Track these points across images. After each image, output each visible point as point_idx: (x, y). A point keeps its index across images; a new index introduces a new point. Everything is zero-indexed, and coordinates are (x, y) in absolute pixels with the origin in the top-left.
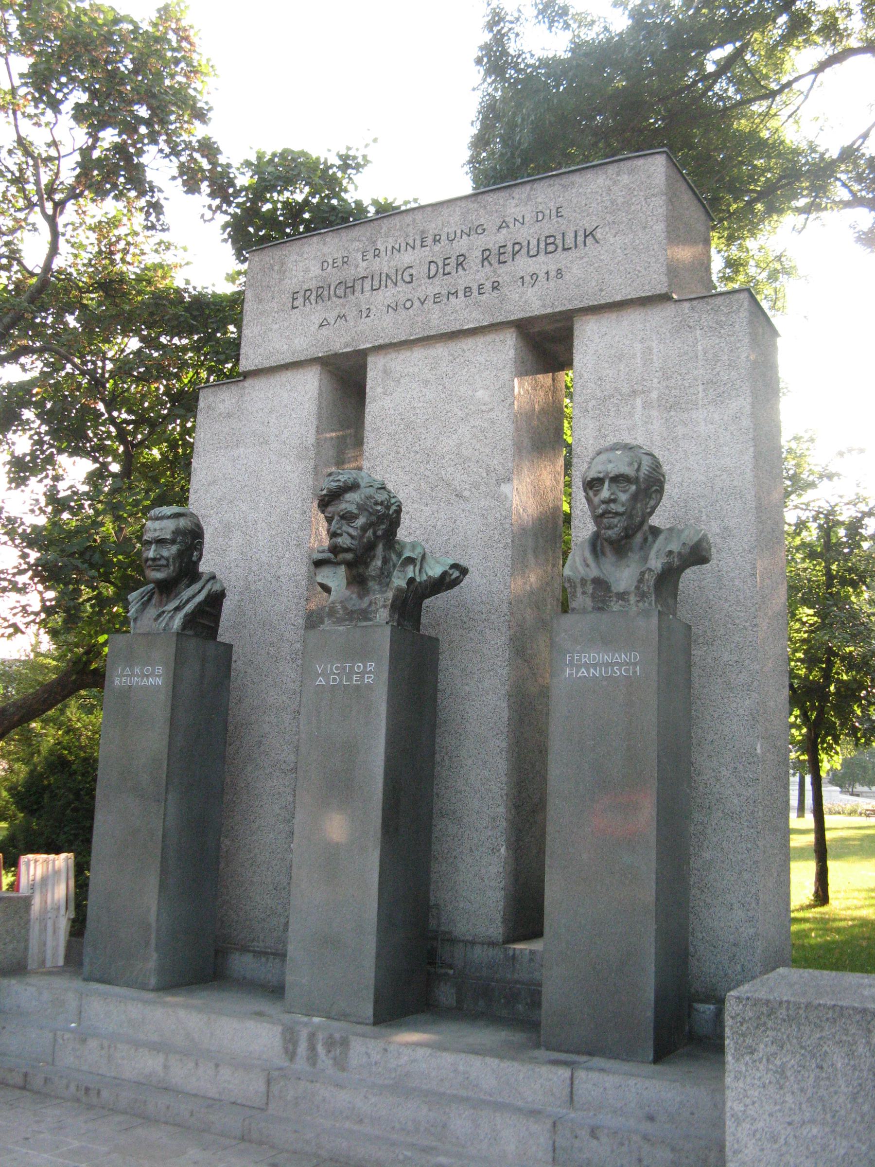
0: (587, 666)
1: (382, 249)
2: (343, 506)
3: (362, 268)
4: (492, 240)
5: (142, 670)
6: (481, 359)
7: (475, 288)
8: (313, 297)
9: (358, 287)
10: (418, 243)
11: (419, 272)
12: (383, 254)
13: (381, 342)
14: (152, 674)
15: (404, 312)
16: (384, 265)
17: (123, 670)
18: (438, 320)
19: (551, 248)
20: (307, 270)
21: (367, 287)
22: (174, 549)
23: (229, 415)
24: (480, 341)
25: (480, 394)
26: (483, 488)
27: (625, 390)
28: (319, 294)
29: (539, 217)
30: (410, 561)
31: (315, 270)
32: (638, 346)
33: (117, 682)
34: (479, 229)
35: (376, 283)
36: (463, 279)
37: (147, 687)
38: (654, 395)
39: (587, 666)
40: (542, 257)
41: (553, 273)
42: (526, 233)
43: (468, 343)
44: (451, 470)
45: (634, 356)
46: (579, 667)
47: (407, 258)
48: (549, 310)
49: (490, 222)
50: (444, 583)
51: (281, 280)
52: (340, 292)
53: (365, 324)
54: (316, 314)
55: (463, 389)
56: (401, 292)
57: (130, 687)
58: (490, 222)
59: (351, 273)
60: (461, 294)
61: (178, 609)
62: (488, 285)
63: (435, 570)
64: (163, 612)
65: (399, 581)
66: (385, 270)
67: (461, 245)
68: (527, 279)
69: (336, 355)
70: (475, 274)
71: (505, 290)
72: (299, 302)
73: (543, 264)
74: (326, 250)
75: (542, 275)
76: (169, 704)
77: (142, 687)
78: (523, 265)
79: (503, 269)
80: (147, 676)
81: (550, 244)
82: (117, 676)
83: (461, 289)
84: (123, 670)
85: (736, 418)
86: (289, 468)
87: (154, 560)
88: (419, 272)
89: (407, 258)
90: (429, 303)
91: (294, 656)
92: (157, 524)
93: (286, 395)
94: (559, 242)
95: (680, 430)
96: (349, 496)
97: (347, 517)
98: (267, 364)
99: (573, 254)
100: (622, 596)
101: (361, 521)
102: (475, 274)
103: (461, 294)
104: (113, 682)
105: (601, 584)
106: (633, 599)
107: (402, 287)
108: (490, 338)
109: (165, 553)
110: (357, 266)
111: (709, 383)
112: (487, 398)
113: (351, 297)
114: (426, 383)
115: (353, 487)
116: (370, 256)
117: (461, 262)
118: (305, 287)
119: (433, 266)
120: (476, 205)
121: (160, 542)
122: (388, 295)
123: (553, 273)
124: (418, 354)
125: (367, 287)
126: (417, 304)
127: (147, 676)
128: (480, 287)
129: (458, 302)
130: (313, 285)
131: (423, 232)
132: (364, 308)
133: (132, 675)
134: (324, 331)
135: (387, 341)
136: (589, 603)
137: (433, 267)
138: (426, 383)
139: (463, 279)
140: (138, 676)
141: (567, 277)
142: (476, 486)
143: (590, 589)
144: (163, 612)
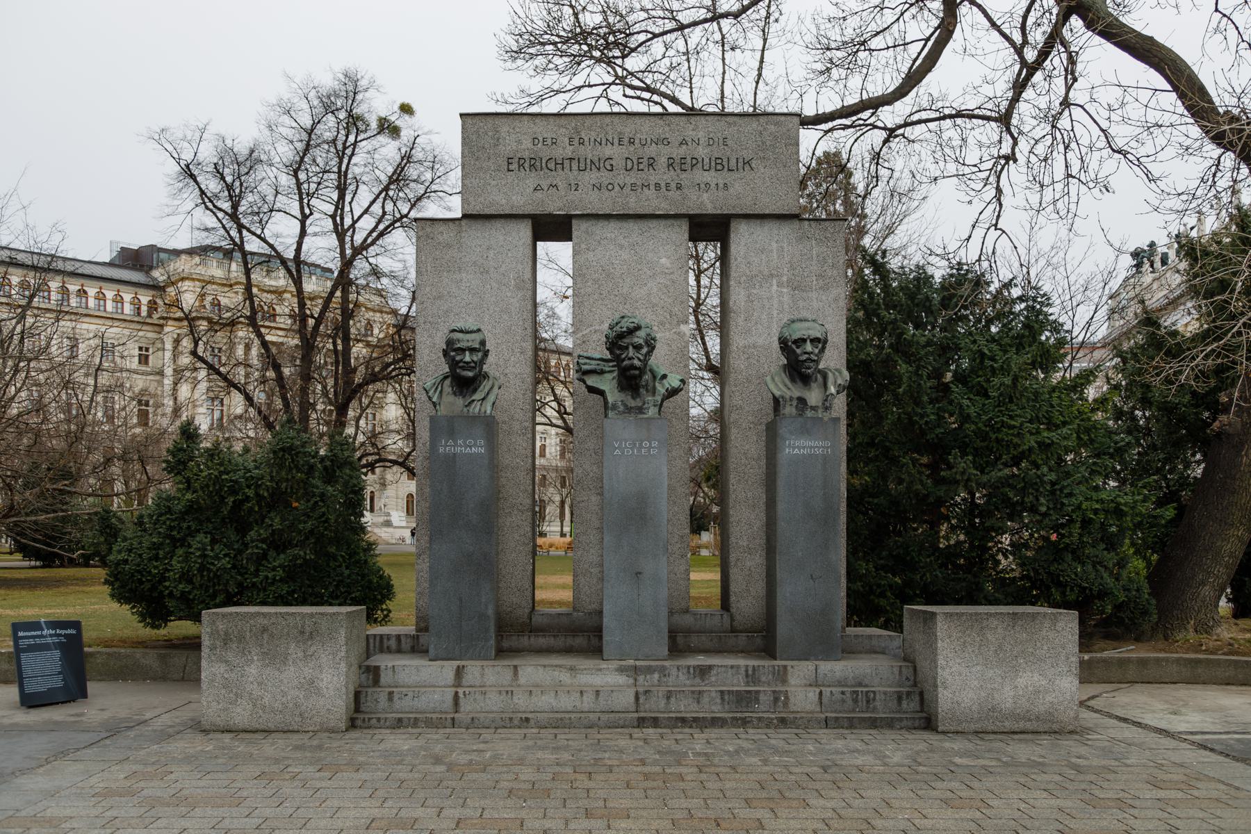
0: (799, 448)
1: (586, 139)
2: (636, 340)
3: (569, 151)
4: (678, 152)
6: (664, 236)
7: (663, 185)
8: (527, 165)
9: (567, 163)
10: (616, 141)
11: (618, 162)
12: (587, 143)
13: (589, 211)
14: (475, 445)
15: (607, 193)
16: (588, 152)
18: (634, 204)
19: (719, 167)
20: (519, 142)
21: (575, 166)
22: (480, 354)
23: (449, 246)
24: (663, 222)
25: (663, 260)
26: (667, 326)
27: (766, 272)
28: (533, 164)
29: (710, 142)
30: (664, 376)
31: (527, 143)
32: (775, 245)
33: (441, 450)
34: (665, 141)
35: (582, 166)
36: (653, 178)
38: (785, 279)
39: (799, 448)
40: (712, 173)
41: (721, 186)
42: (702, 152)
43: (653, 223)
44: (643, 311)
45: (772, 251)
46: (794, 448)
47: (608, 151)
48: (719, 212)
49: (675, 138)
50: (673, 392)
51: (496, 145)
52: (552, 165)
53: (574, 196)
54: (531, 180)
55: (650, 255)
56: (604, 177)
58: (675, 138)
59: (558, 153)
60: (652, 187)
61: (483, 399)
62: (673, 185)
63: (676, 384)
65: (661, 390)
66: (590, 156)
67: (652, 150)
68: (702, 186)
69: (551, 215)
70: (661, 175)
71: (685, 191)
72: (514, 166)
73: (710, 177)
74: (535, 129)
75: (713, 186)
78: (700, 176)
79: (684, 175)
81: (719, 164)
83: (652, 183)
85: (836, 300)
86: (509, 294)
87: (467, 363)
88: (618, 162)
89: (608, 151)
90: (627, 190)
92: (468, 336)
93: (502, 238)
94: (725, 163)
95: (801, 304)
96: (638, 333)
97: (638, 348)
98: (487, 211)
99: (735, 175)
100: (814, 408)
101: (645, 350)
102: (661, 175)
103: (652, 187)
105: (802, 401)
106: (820, 411)
107: (604, 173)
108: (669, 222)
109: (475, 359)
110: (564, 148)
111: (820, 276)
112: (669, 265)
113: (560, 172)
114: (621, 247)
115: (638, 328)
116: (576, 142)
117: (652, 163)
118: (519, 155)
119: (629, 162)
120: (661, 122)
121: (472, 350)
122: (592, 177)
123: (721, 186)
124: (613, 224)
125: (575, 166)
126: (617, 188)
128: (667, 185)
129: (650, 193)
130: (526, 155)
131: (620, 133)
132: (573, 183)
134: (539, 194)
135: (594, 212)
136: (794, 410)
137: (629, 162)
138: (621, 247)
139: (653, 178)
141: (731, 190)
142: (662, 324)
143: (795, 403)
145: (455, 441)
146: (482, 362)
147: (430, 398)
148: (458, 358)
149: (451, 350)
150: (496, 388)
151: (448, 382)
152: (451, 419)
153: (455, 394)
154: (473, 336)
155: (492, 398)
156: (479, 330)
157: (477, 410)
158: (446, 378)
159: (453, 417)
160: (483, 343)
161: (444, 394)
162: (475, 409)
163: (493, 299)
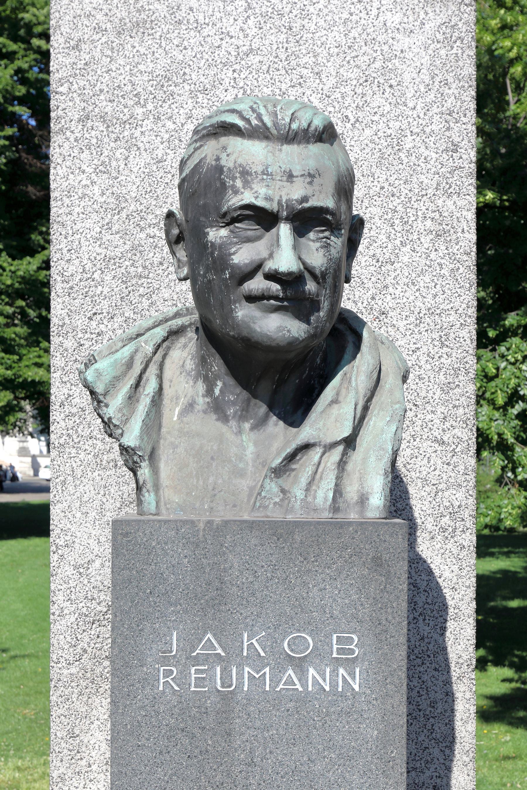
5: (272, 644)
17: (190, 642)
37: (302, 700)
57: (227, 698)
64: (306, 447)
76: (398, 753)
77: (277, 699)
80: (300, 665)
82: (165, 661)
84: (190, 642)
91: (446, 520)
104: (150, 681)
109: (317, 259)
121: (306, 220)
127: (300, 665)
133: (231, 658)
140: (258, 662)
144: (306, 447)
145: (227, 634)
146: (337, 275)
147: (109, 428)
148: (242, 256)
149: (202, 211)
150: (390, 380)
151: (184, 354)
152: (212, 539)
153: (218, 408)
154: (312, 154)
155: (379, 429)
156: (327, 135)
157: (324, 492)
158: (174, 334)
159: (220, 530)
160: (345, 189)
161: (172, 414)
162: (313, 490)
163: (336, 36)
